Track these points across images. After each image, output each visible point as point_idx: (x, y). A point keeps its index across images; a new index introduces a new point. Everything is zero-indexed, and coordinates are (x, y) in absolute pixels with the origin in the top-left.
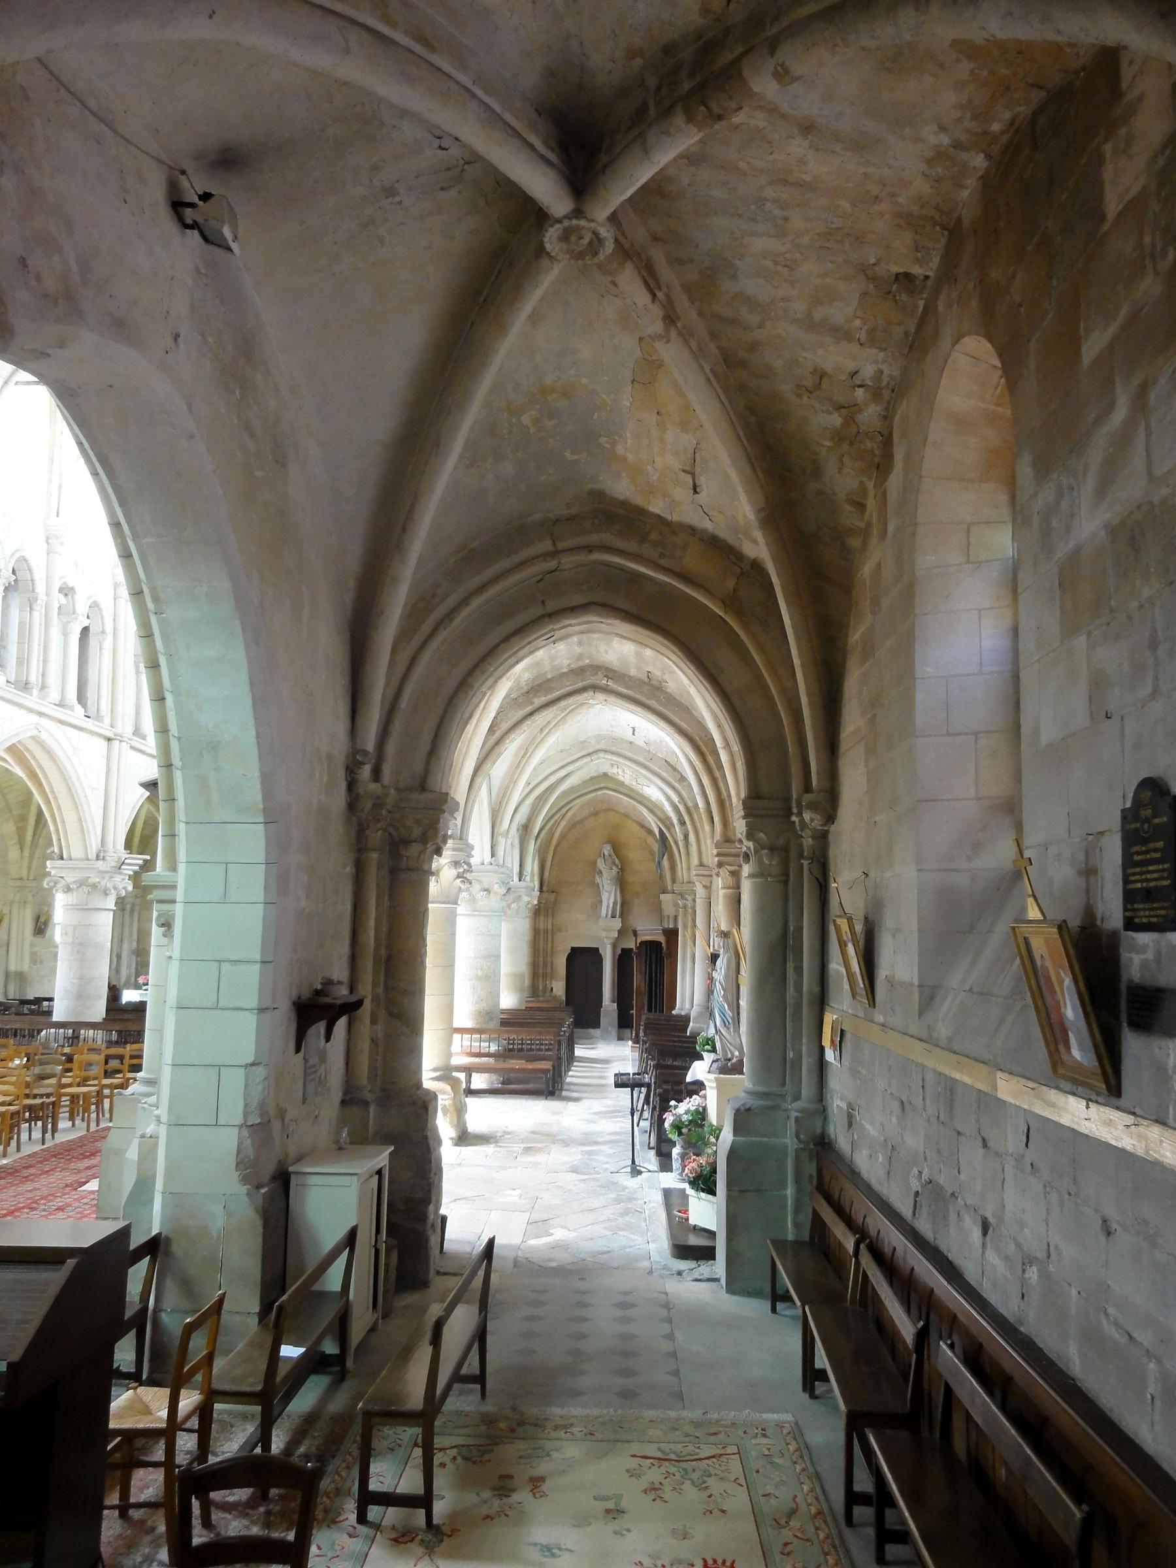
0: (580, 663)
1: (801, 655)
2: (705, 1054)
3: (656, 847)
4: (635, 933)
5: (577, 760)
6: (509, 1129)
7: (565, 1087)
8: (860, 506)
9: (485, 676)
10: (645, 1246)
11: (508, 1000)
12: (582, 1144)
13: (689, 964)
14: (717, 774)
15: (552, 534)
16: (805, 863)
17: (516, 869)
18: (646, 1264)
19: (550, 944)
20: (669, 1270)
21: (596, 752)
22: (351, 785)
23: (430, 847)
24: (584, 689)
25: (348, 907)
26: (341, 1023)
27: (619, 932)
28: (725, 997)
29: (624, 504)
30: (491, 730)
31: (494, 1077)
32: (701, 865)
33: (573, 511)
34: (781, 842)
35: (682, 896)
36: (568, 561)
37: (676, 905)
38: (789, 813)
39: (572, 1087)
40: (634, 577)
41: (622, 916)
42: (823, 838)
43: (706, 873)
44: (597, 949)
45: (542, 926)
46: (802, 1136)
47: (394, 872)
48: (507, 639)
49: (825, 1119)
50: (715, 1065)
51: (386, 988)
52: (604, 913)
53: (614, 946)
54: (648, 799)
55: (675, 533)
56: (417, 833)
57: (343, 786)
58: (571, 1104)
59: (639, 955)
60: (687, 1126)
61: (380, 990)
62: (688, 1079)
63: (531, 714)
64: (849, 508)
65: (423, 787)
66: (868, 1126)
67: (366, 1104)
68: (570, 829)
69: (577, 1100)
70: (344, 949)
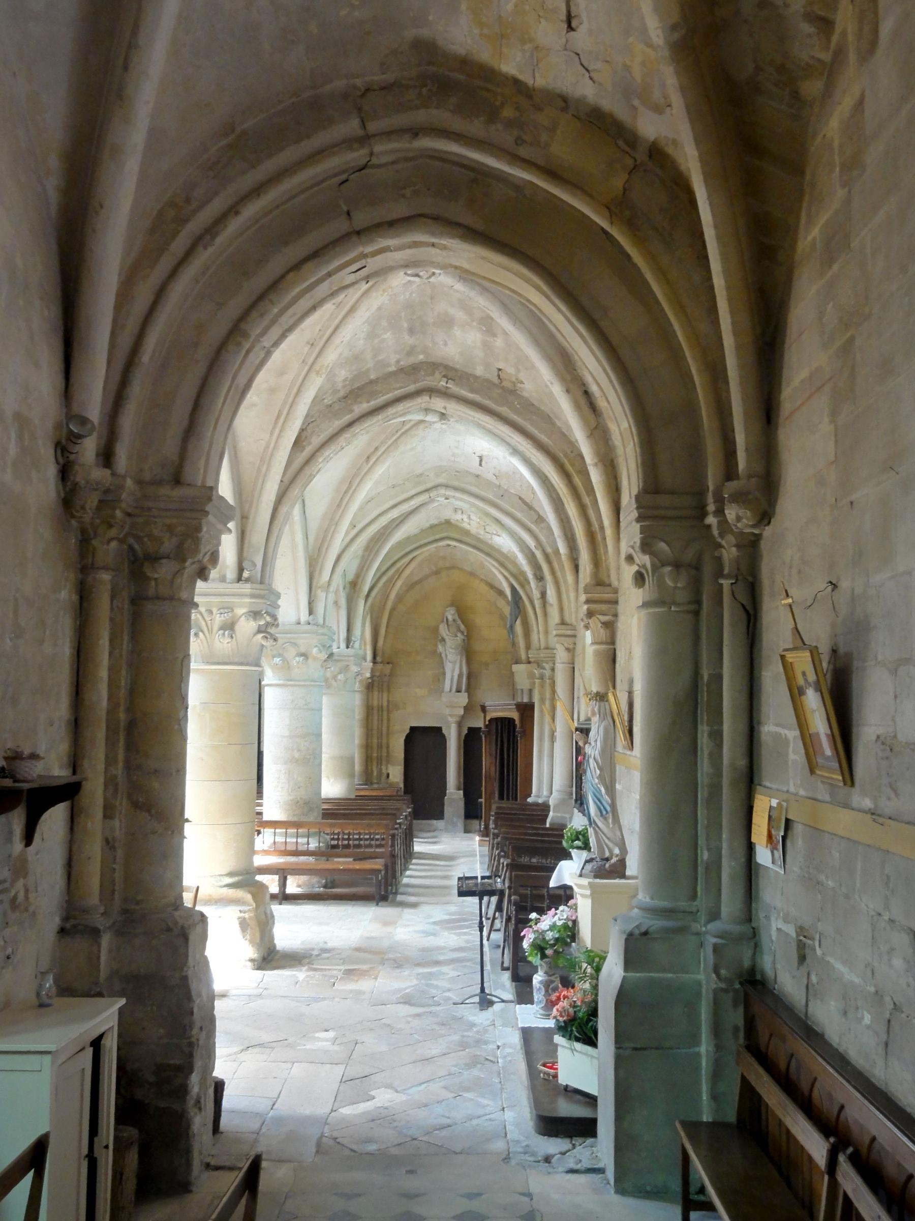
0: (412, 360)
1: (726, 271)
2: (574, 852)
3: (507, 611)
4: (484, 709)
5: (412, 497)
6: (330, 945)
7: (401, 890)
8: (825, 24)
9: (266, 321)
10: (497, 1115)
11: (333, 787)
12: (418, 965)
14: (587, 500)
15: (360, 109)
16: (726, 583)
17: (343, 634)
18: (499, 1145)
20: (533, 1154)
21: (436, 487)
22: (65, 472)
23: (190, 567)
24: (418, 393)
25: (66, 650)
26: (55, 819)
27: (466, 708)
28: (601, 778)
29: (465, 63)
30: (298, 443)
31: (315, 879)
32: (563, 623)
33: (389, 77)
34: (689, 556)
35: (539, 665)
36: (384, 149)
37: (531, 676)
38: (704, 514)
39: (410, 890)
40: (480, 174)
41: (468, 690)
42: (751, 546)
43: (569, 632)
44: (438, 730)
45: (375, 703)
46: (723, 972)
47: (137, 600)
48: (297, 267)
49: (757, 947)
50: (589, 867)
51: (128, 766)
53: (460, 725)
55: (538, 108)
56: (168, 544)
57: (51, 470)
58: (407, 911)
59: (488, 733)
60: (553, 946)
61: (119, 770)
62: (552, 884)
63: (350, 425)
64: (806, 28)
65: (177, 480)
66: (839, 966)
67: (95, 933)
68: (408, 591)
69: (414, 905)
70: (62, 709)
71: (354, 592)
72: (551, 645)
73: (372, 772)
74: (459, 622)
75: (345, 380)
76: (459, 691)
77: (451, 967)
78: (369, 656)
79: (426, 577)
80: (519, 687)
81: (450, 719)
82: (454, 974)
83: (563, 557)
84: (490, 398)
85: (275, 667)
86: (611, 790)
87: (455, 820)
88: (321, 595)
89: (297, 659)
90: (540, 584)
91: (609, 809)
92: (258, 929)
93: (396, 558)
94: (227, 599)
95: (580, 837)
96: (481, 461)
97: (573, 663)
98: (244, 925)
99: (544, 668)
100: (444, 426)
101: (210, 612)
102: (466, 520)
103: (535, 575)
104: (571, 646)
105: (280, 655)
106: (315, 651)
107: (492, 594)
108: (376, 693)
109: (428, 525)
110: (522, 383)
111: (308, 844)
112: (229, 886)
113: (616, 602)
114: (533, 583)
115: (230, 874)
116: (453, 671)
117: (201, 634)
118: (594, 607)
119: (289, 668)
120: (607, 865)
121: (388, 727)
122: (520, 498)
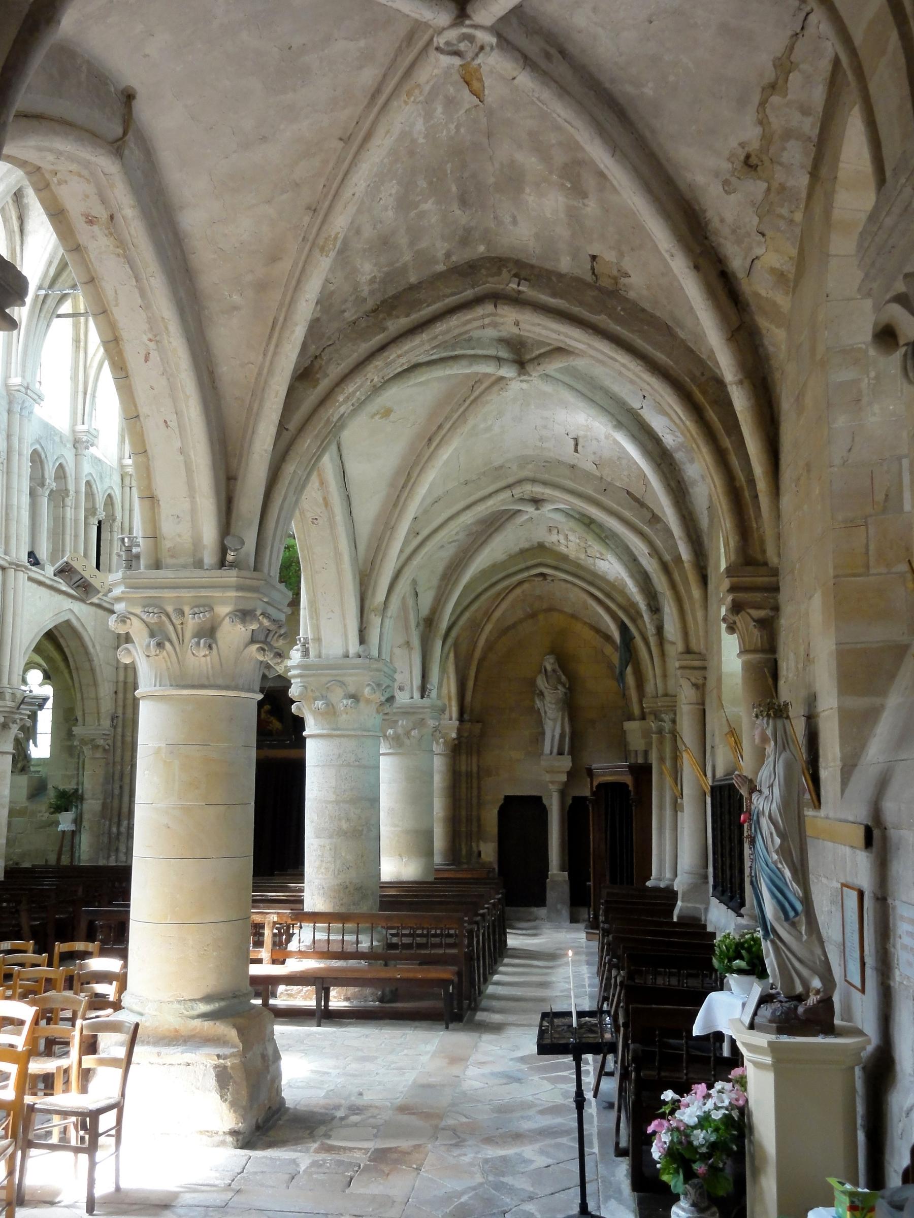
4: (590, 773)
5: (490, 496)
6: (368, 1098)
7: (484, 1003)
11: (395, 867)
12: (489, 1140)
13: (668, 813)
14: (727, 443)
17: (417, 681)
19: (475, 792)
21: (520, 482)
24: (478, 301)
27: (569, 774)
28: (784, 851)
31: (368, 991)
32: (688, 651)
37: (647, 734)
39: (495, 1003)
41: (572, 752)
43: (697, 663)
44: (538, 800)
45: (463, 768)
50: (766, 1012)
52: (547, 749)
53: (563, 793)
54: (603, 579)
58: (487, 1037)
60: (705, 1157)
62: (696, 1031)
63: (383, 348)
69: (497, 1028)
71: (430, 631)
72: (671, 691)
73: (460, 850)
74: (560, 673)
75: (372, 281)
76: (560, 753)
77: (537, 1146)
78: (455, 715)
79: (521, 621)
80: (632, 747)
81: (551, 786)
82: (541, 1161)
83: (687, 565)
84: (581, 303)
85: (317, 713)
86: (801, 873)
87: (559, 906)
88: (376, 621)
89: (345, 701)
90: (655, 617)
91: (799, 907)
92: (245, 1083)
93: (480, 590)
94: (204, 593)
95: (743, 952)
96: (576, 445)
97: (703, 704)
98: (223, 1078)
99: (662, 720)
100: (525, 386)
101: (181, 613)
102: (562, 541)
103: (649, 606)
104: (700, 682)
105: (323, 697)
106: (367, 691)
107: (598, 641)
108: (464, 757)
109: (517, 549)
110: (627, 275)
111: (358, 942)
112: (205, 1016)
113: (776, 589)
114: (646, 617)
115: (207, 999)
116: (553, 731)
117: (167, 644)
118: (742, 596)
119: (335, 713)
120: (801, 1010)
121: (479, 797)
122: (628, 492)
